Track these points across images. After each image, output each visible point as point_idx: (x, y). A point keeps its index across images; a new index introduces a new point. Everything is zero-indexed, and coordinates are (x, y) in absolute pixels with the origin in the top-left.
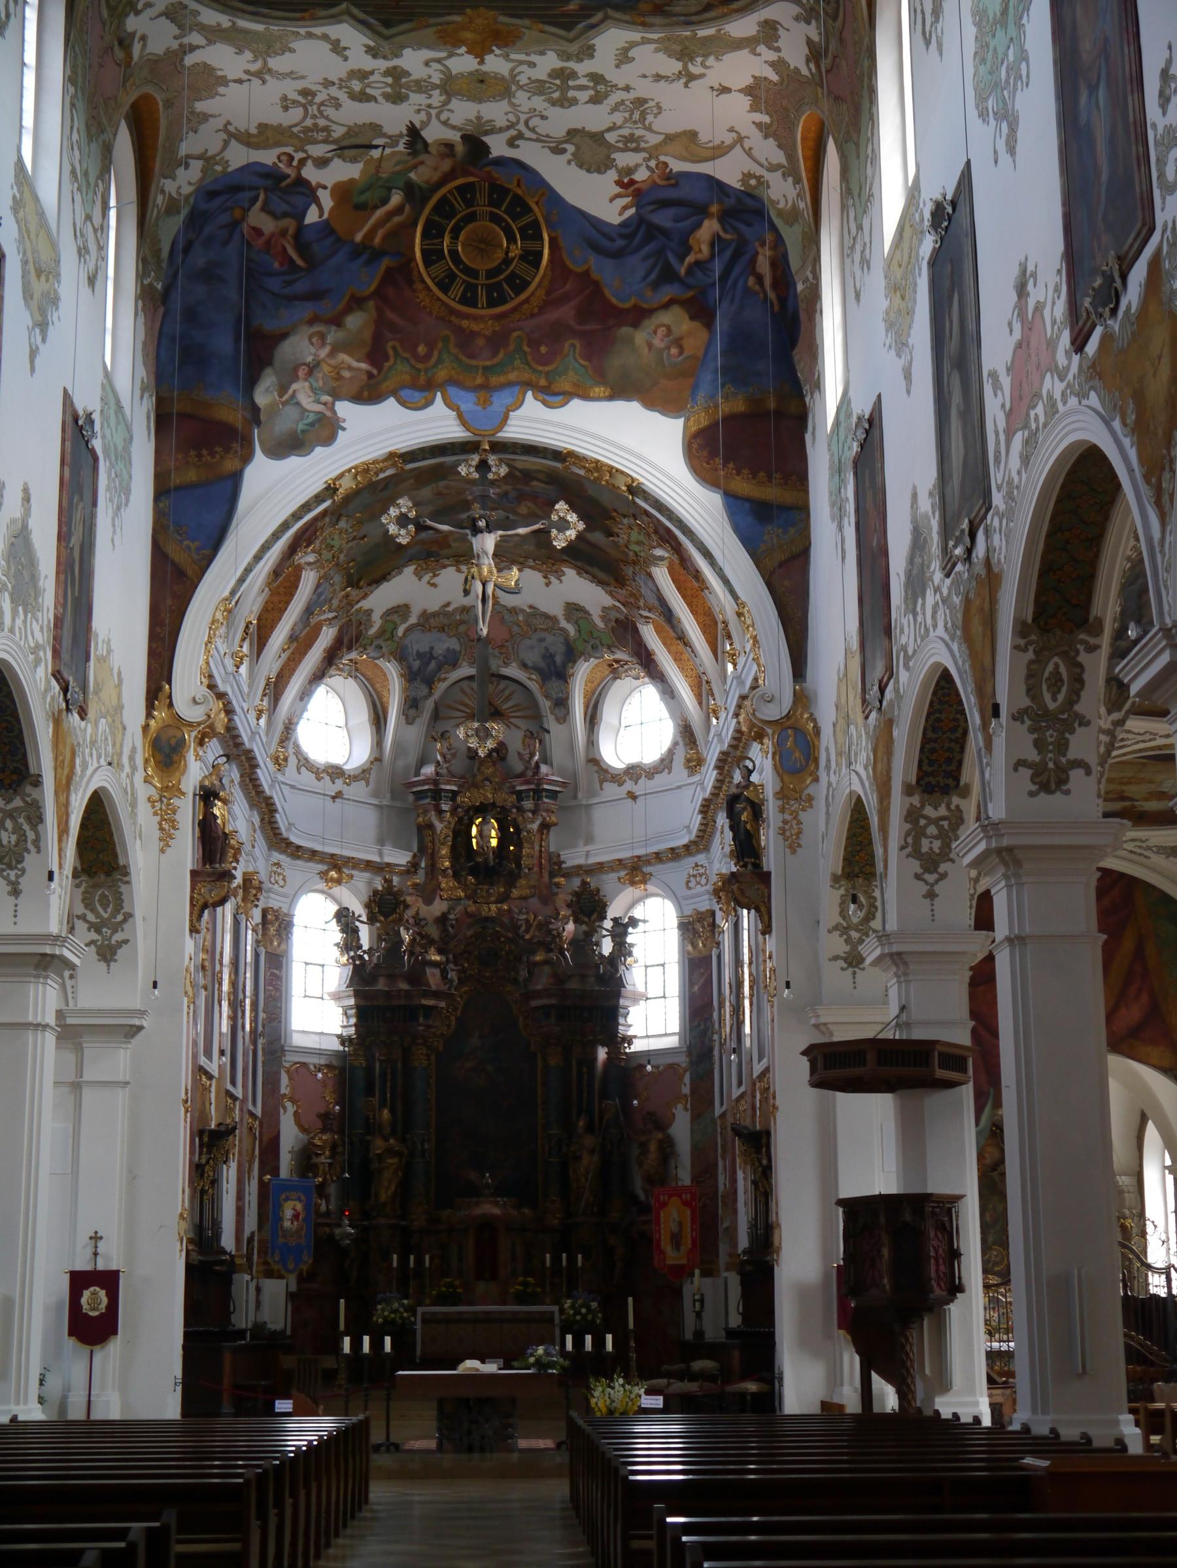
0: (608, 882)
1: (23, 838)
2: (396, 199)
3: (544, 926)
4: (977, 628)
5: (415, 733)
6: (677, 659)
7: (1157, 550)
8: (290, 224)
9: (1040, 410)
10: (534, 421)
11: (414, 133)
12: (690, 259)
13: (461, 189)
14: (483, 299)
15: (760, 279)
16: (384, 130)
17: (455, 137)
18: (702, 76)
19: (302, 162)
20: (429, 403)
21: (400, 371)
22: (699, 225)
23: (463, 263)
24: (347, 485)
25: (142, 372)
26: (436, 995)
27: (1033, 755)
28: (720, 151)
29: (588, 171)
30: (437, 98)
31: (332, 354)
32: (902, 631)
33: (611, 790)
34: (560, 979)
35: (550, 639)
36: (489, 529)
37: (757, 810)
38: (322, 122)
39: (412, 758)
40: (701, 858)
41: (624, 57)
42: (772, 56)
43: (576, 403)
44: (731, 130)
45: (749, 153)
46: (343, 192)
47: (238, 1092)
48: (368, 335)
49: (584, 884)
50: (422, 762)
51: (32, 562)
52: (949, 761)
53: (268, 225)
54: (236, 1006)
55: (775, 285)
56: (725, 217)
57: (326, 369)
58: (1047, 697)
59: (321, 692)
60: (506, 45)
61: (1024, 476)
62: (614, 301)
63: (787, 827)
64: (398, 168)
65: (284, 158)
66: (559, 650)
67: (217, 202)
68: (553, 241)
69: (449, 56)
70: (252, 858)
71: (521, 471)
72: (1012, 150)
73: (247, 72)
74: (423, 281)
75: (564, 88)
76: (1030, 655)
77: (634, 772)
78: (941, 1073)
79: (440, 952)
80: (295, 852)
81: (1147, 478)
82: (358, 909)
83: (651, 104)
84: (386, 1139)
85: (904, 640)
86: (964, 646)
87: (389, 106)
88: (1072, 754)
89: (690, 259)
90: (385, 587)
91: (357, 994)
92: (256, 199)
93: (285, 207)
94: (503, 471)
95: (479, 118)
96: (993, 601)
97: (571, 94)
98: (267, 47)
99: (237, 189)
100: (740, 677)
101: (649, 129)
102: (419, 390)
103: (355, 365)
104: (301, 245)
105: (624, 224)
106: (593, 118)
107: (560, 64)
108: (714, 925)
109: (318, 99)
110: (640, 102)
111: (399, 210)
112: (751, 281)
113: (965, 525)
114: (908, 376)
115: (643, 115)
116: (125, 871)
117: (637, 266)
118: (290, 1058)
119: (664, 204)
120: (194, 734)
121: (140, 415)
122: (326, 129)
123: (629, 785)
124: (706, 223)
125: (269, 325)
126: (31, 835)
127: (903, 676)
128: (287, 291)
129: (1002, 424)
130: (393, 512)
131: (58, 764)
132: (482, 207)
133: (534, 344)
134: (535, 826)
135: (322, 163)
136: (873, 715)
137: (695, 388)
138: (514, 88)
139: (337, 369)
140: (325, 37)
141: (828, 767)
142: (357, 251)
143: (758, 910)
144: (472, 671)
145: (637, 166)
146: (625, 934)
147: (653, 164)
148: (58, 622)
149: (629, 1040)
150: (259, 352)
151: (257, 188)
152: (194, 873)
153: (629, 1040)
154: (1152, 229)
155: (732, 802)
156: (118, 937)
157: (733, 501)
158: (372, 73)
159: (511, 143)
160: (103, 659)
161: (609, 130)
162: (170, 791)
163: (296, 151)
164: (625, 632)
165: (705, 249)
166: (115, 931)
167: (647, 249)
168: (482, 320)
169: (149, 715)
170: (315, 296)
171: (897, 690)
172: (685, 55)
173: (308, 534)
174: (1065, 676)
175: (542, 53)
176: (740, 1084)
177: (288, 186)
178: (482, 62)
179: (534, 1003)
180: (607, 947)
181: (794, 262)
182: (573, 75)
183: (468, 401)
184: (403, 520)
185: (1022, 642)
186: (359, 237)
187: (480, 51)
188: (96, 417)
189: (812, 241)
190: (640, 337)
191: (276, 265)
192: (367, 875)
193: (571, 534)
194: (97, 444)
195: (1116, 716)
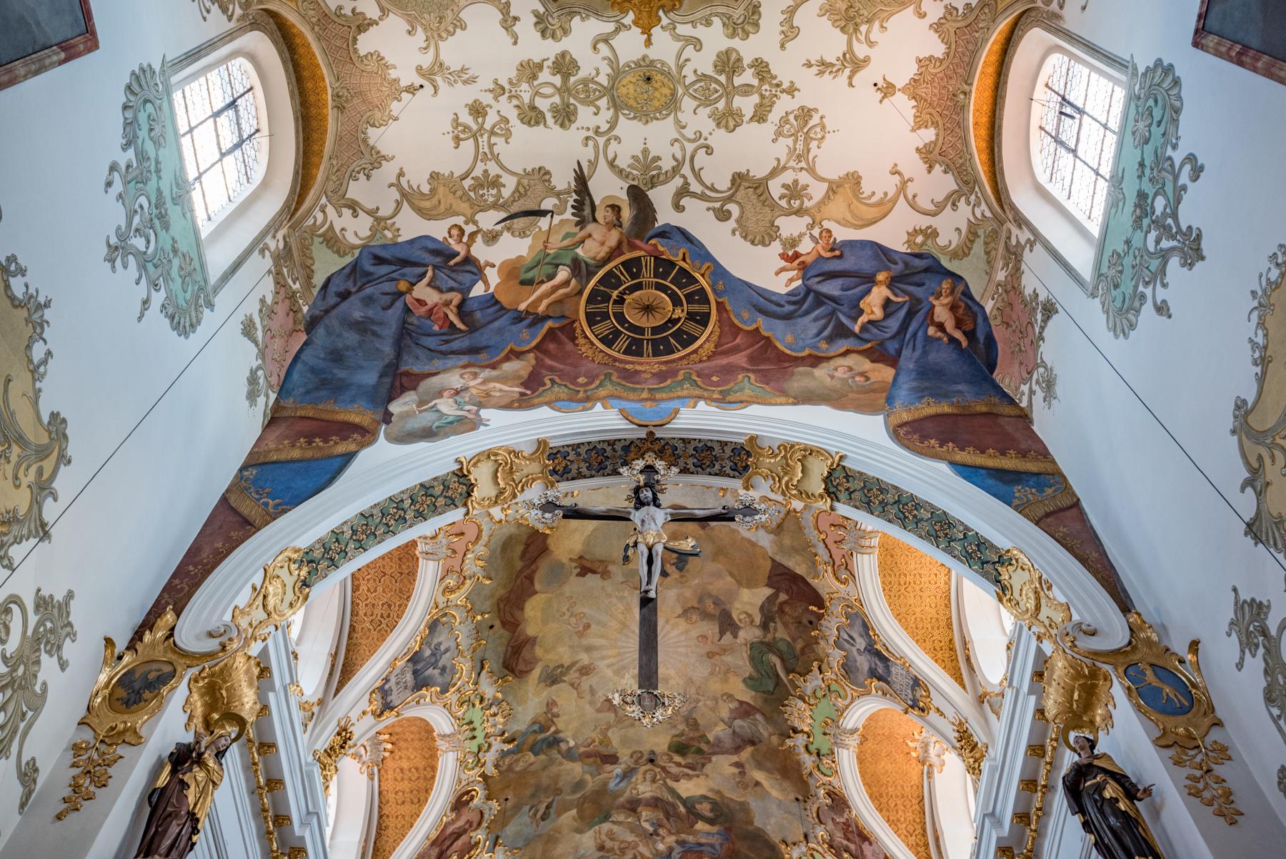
2: (563, 274)
8: (456, 298)
11: (582, 181)
12: (863, 319)
13: (627, 265)
14: (648, 348)
15: (941, 327)
16: (554, 181)
18: (867, 60)
19: (473, 236)
22: (868, 291)
28: (885, 207)
29: (753, 243)
38: (494, 170)
44: (895, 172)
53: (432, 297)
55: (959, 324)
56: (892, 283)
60: (673, 8)
62: (788, 352)
63: (1201, 786)
64: (566, 243)
65: (455, 232)
67: (384, 269)
69: (617, 31)
71: (684, 802)
73: (419, 69)
74: (586, 337)
75: (730, 91)
83: (815, 120)
89: (863, 319)
92: (423, 275)
93: (452, 284)
95: (645, 152)
97: (738, 102)
99: (405, 263)
100: (993, 814)
101: (811, 170)
106: (755, 148)
107: (725, 43)
109: (488, 126)
110: (805, 114)
111: (566, 283)
112: (931, 331)
115: (808, 139)
117: (809, 326)
120: (194, 671)
122: (496, 183)
124: (875, 289)
128: (443, 348)
132: (647, 276)
135: (492, 238)
138: (680, 91)
142: (519, 318)
145: (801, 235)
147: (816, 232)
151: (426, 265)
155: (1075, 787)
158: (540, 67)
159: (678, 208)
161: (774, 173)
163: (466, 223)
165: (878, 314)
167: (817, 312)
168: (649, 364)
170: (473, 351)
173: (459, 843)
175: (708, 23)
177: (456, 264)
178: (648, 43)
186: (522, 307)
191: (436, 328)
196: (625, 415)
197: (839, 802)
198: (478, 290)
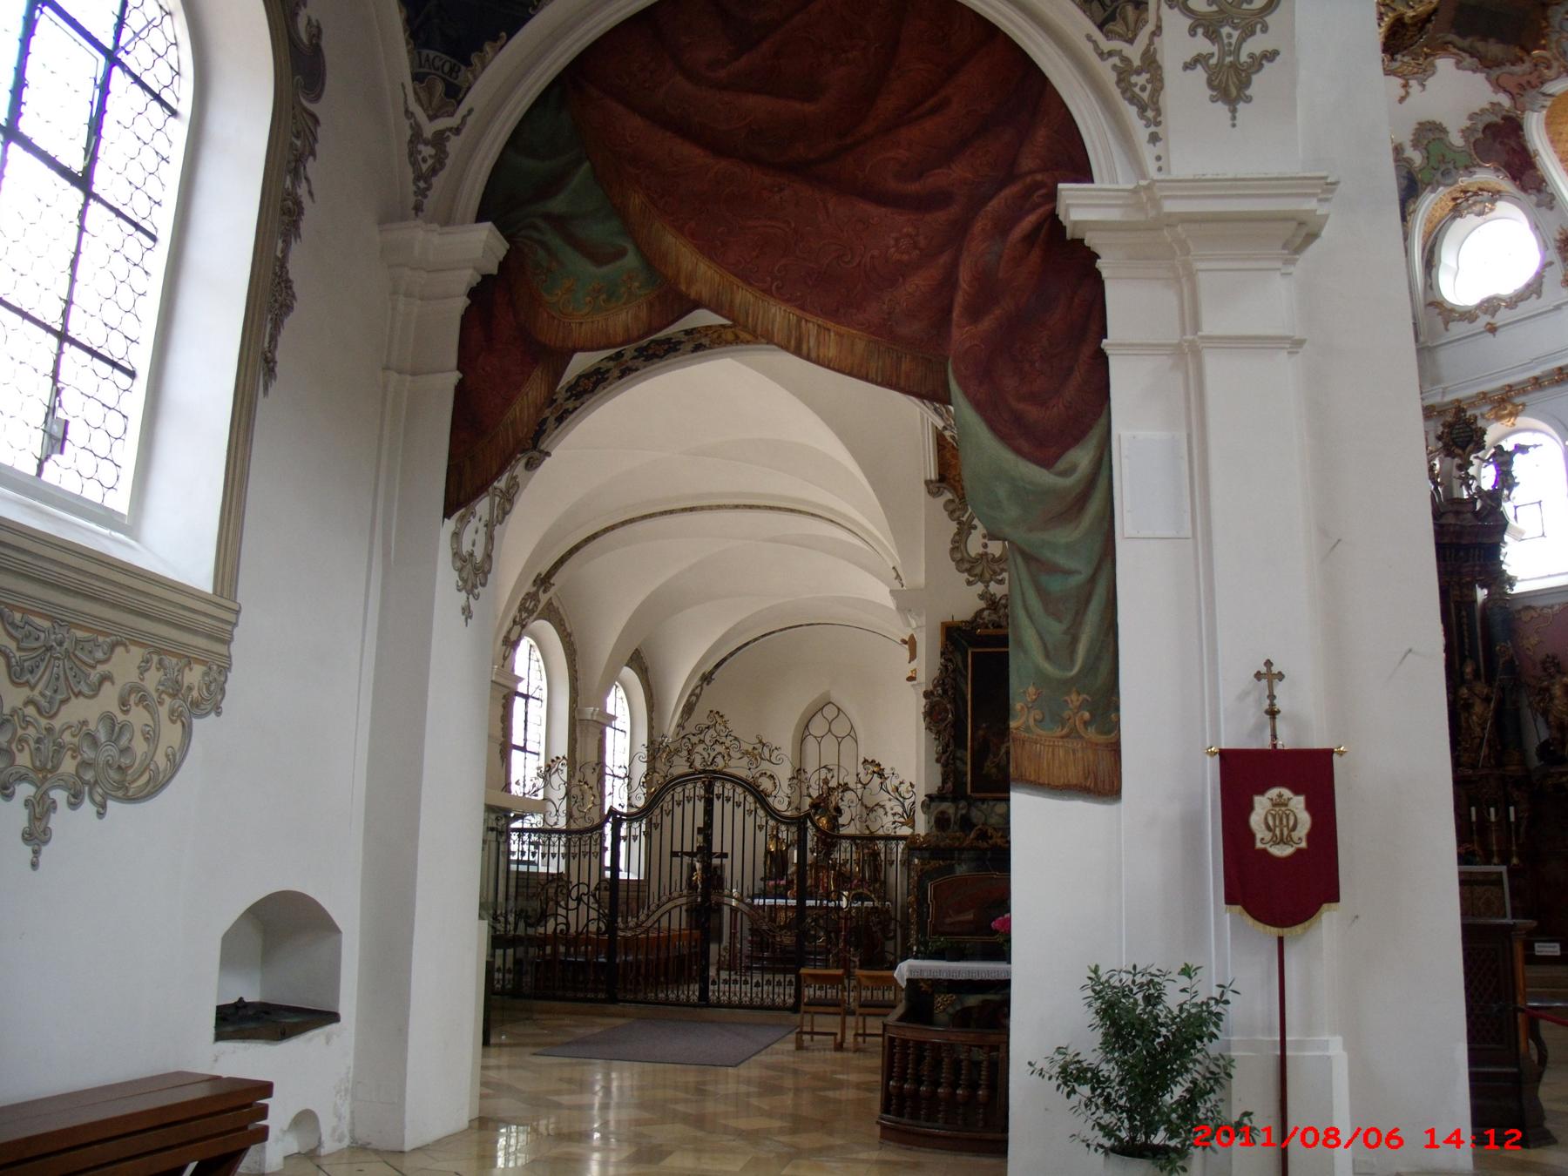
33: (1458, 329)
146: (1510, 463)
149: (1511, 581)
166: (1249, 32)
180: (1487, 477)
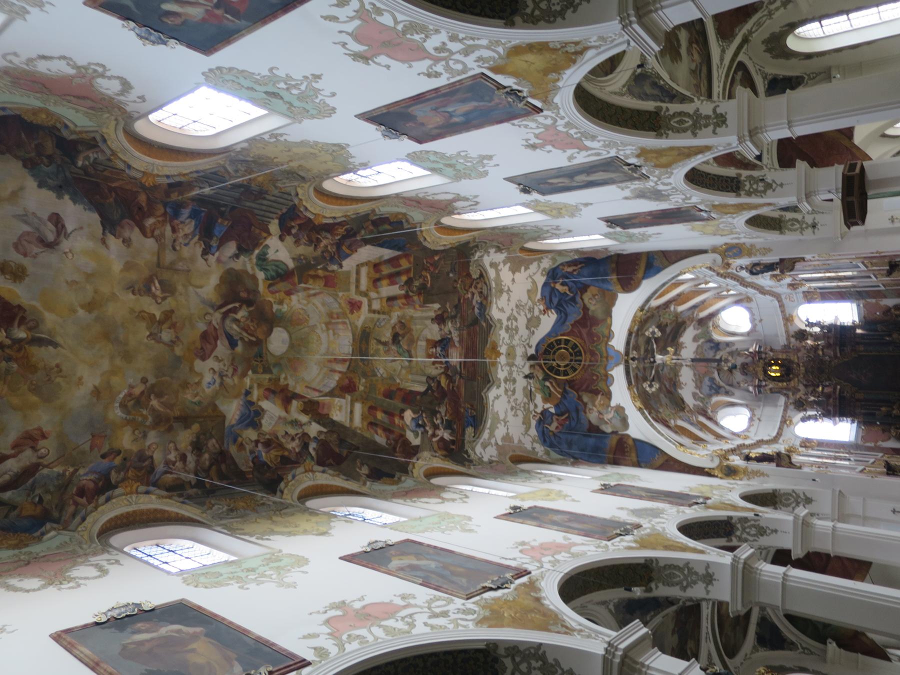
0: (792, 329)
1: (754, 526)
2: (547, 384)
3: (808, 351)
4: (664, 160)
5: (737, 392)
6: (711, 305)
7: (600, 50)
8: (555, 417)
9: (572, 132)
10: (618, 342)
11: (526, 377)
14: (579, 358)
15: (574, 270)
17: (528, 364)
20: (612, 376)
21: (601, 385)
23: (569, 365)
24: (639, 404)
25: (598, 468)
26: (835, 389)
27: (711, 128)
28: (534, 282)
30: (514, 368)
31: (595, 406)
32: (677, 202)
33: (759, 328)
34: (828, 346)
35: (705, 347)
36: (654, 357)
37: (755, 265)
39: (746, 394)
40: (783, 297)
41: (502, 310)
42: (502, 265)
43: (613, 328)
45: (534, 274)
46: (545, 400)
47: (872, 460)
48: (590, 395)
49: (792, 336)
50: (748, 391)
51: (646, 510)
52: (726, 181)
53: (555, 424)
54: (836, 458)
55: (576, 265)
57: (600, 409)
58: (687, 125)
59: (724, 422)
61: (600, 138)
66: (709, 345)
68: (562, 335)
70: (781, 447)
72: (490, 158)
75: (512, 329)
76: (670, 132)
77: (753, 320)
78: (858, 170)
79: (818, 387)
80: (779, 434)
81: (574, 62)
82: (801, 415)
84: (893, 409)
85: (680, 201)
86: (673, 166)
87: (517, 384)
88: (710, 113)
90: (685, 399)
91: (834, 416)
94: (635, 352)
96: (652, 151)
98: (496, 419)
102: (608, 379)
103: (599, 399)
104: (562, 414)
105: (557, 313)
106: (522, 321)
108: (808, 292)
110: (517, 306)
111: (551, 383)
113: (626, 168)
114: (586, 205)
116: (775, 491)
117: (570, 309)
118: (860, 442)
119: (551, 300)
121: (611, 470)
122: (525, 404)
123: (757, 322)
125: (587, 426)
126: (753, 522)
127: (694, 200)
129: (584, 153)
130: (648, 389)
131: (726, 509)
133: (594, 342)
134: (771, 354)
135: (536, 406)
136: (713, 215)
137: (608, 290)
139: (600, 405)
140: (493, 401)
141: (739, 238)
143: (794, 263)
144: (716, 373)
148: (671, 503)
149: (854, 322)
150: (594, 430)
152: (777, 466)
153: (854, 322)
154: (483, 74)
156: (802, 496)
157: (645, 277)
159: (530, 347)
160: (691, 489)
162: (745, 472)
164: (702, 322)
165: (566, 288)
169: (717, 477)
170: (577, 411)
171: (700, 203)
172: (501, 291)
174: (678, 119)
176: (870, 277)
179: (839, 355)
181: (568, 259)
182: (507, 326)
183: (612, 362)
184: (651, 386)
185: (664, 136)
187: (499, 354)
188: (603, 483)
189: (560, 253)
190: (592, 308)
192: (789, 411)
193: (656, 330)
194: (612, 484)
195: (696, 99)
196: (617, 365)
197: (658, 307)
198: (553, 410)
